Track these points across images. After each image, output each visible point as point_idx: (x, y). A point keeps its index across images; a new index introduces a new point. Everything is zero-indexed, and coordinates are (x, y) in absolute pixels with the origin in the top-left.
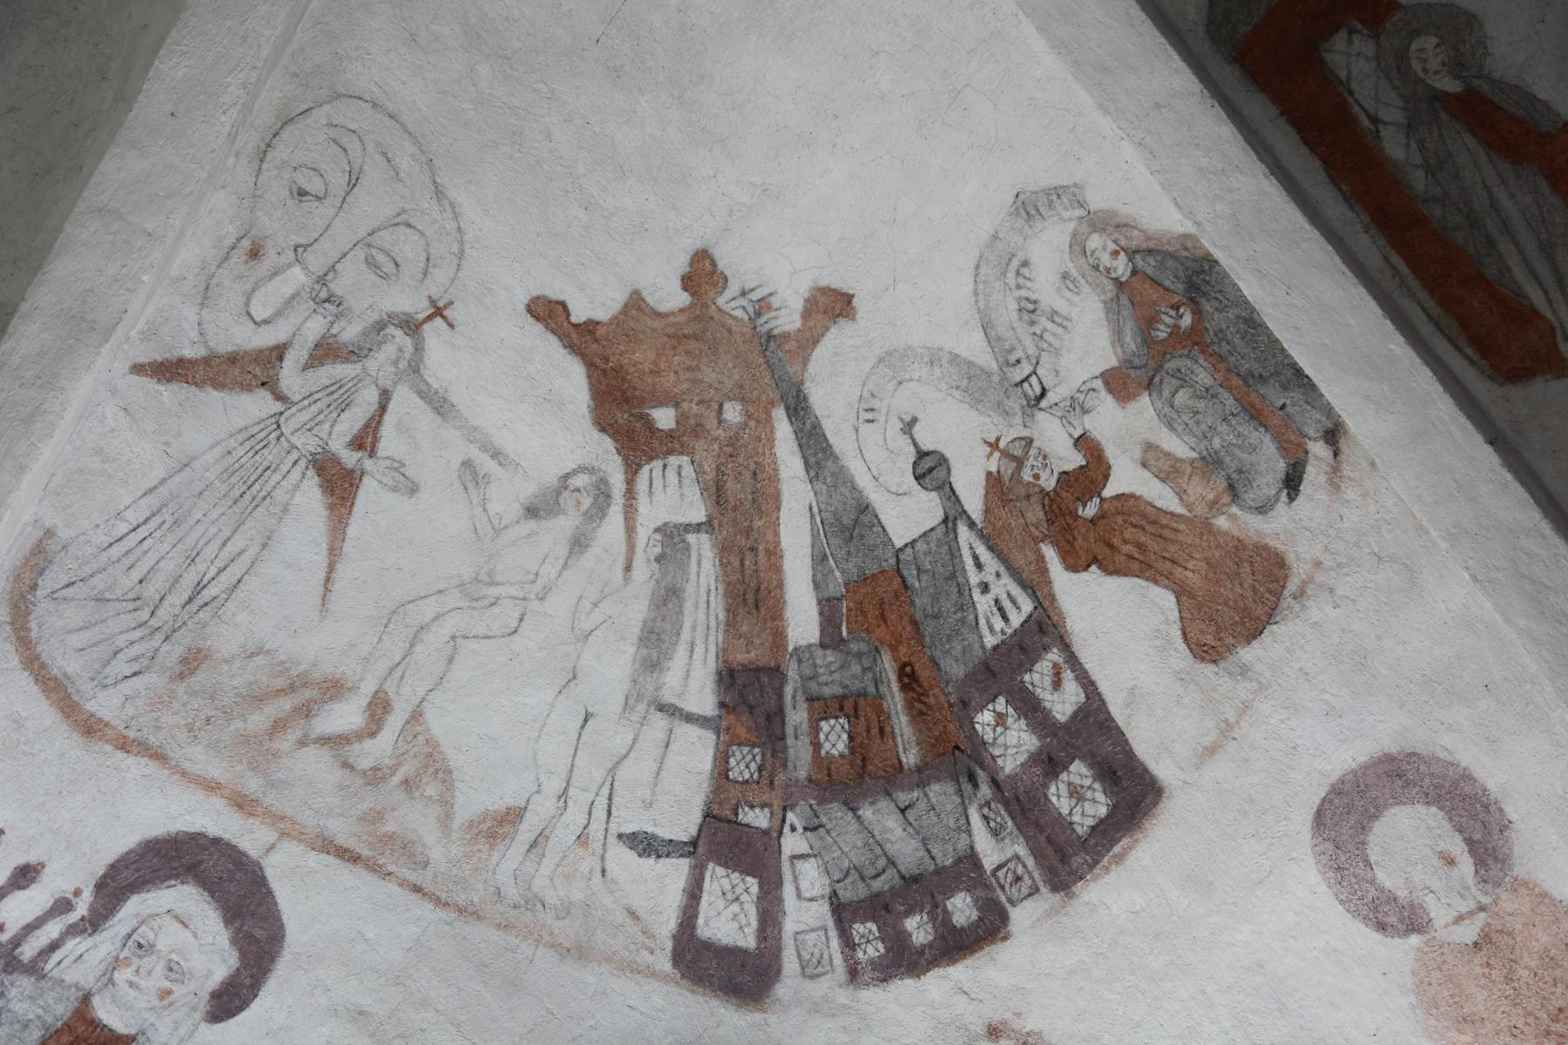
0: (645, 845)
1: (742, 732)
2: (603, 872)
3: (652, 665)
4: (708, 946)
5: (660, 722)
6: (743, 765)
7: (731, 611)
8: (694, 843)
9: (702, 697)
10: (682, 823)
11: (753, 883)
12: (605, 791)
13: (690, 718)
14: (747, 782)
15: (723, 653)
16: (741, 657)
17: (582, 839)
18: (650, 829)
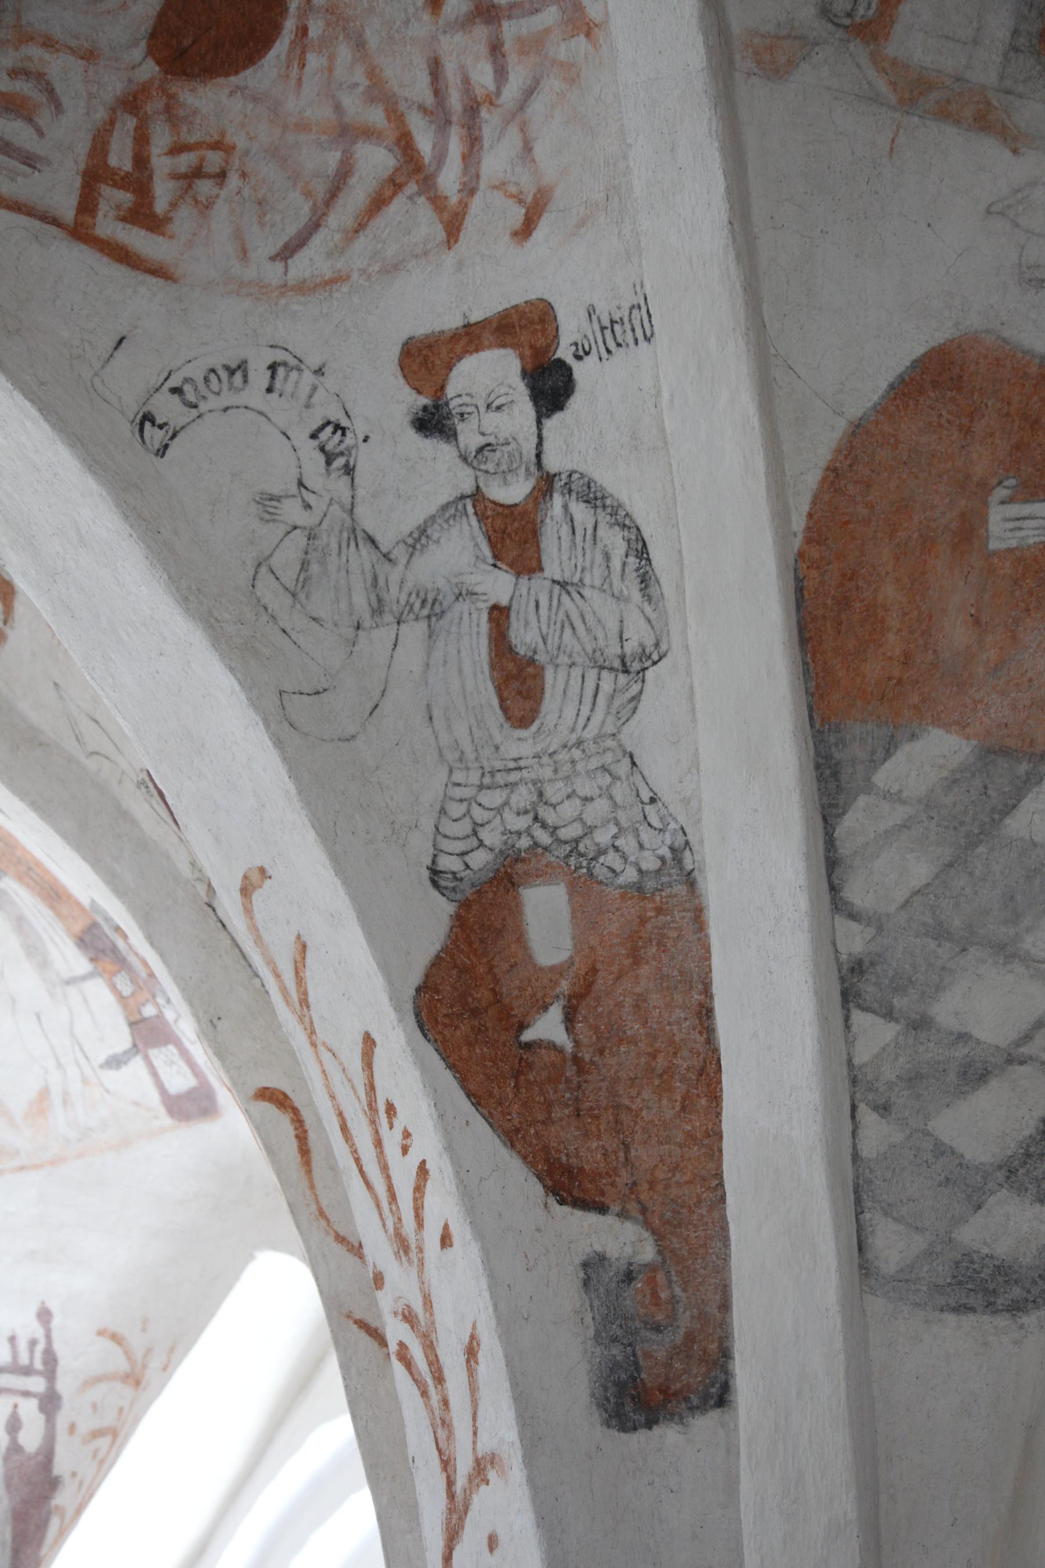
0: (115, 1062)
1: (110, 967)
2: (107, 1091)
3: (44, 965)
4: (179, 1097)
5: (72, 991)
6: (126, 988)
7: (52, 907)
8: (135, 1045)
9: (81, 964)
10: (121, 1039)
11: (171, 1048)
12: (77, 1048)
13: (84, 978)
14: (133, 994)
15: (68, 931)
16: (77, 928)
17: (85, 1081)
18: (111, 1052)
